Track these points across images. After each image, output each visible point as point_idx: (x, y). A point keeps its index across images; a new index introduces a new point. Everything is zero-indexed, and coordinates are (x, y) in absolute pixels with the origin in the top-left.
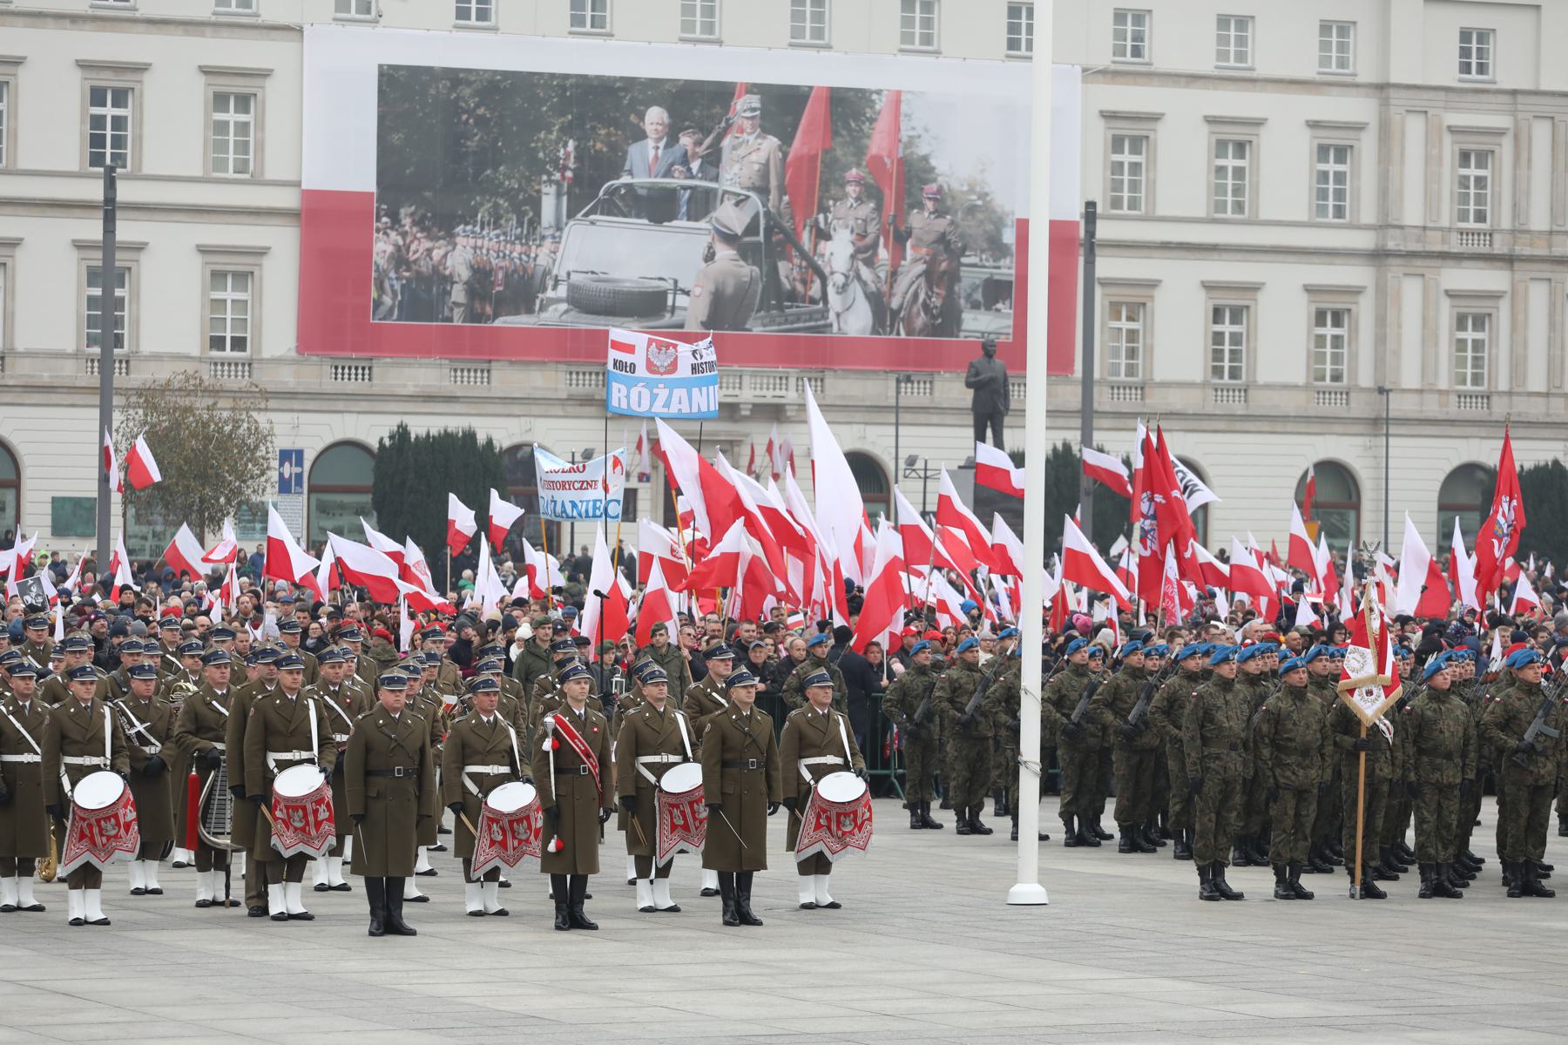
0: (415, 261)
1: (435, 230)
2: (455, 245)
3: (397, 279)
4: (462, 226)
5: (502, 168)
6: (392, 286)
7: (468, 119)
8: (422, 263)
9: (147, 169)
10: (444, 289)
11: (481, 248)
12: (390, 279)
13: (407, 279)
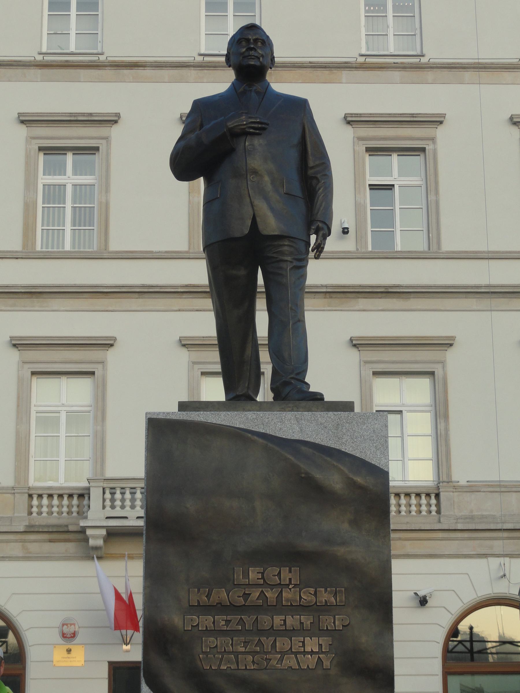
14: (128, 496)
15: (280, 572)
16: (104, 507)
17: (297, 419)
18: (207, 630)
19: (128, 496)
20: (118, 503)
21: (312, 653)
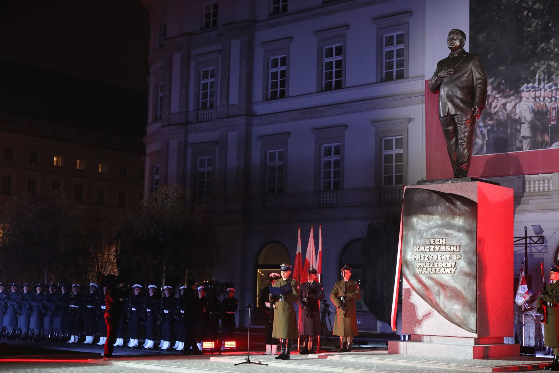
0: (496, 113)
1: (508, 90)
2: (521, 99)
3: (484, 126)
4: (525, 85)
5: (552, 41)
6: (481, 132)
7: (527, 14)
8: (500, 113)
9: (347, 86)
10: (516, 129)
11: (539, 97)
12: (480, 127)
13: (491, 125)
15: (440, 240)
17: (449, 185)
18: (418, 260)
21: (449, 268)
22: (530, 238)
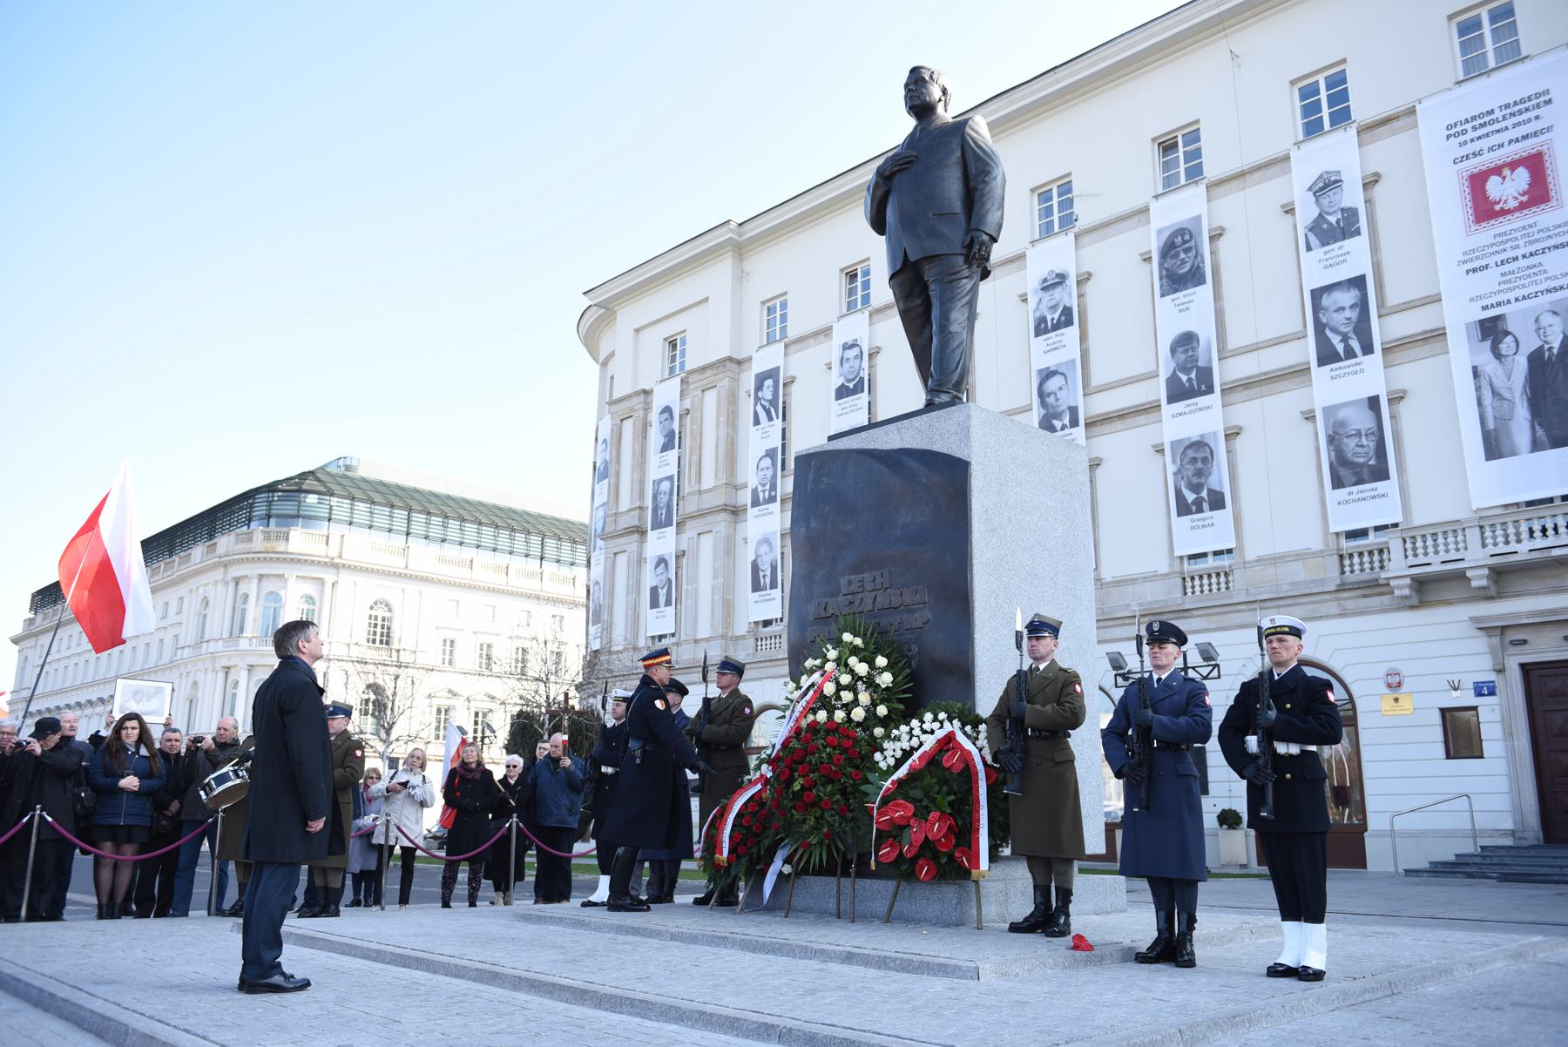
14: (1430, 542)
16: (1406, 557)
19: (1430, 542)
20: (1420, 551)
22: (1193, 668)
